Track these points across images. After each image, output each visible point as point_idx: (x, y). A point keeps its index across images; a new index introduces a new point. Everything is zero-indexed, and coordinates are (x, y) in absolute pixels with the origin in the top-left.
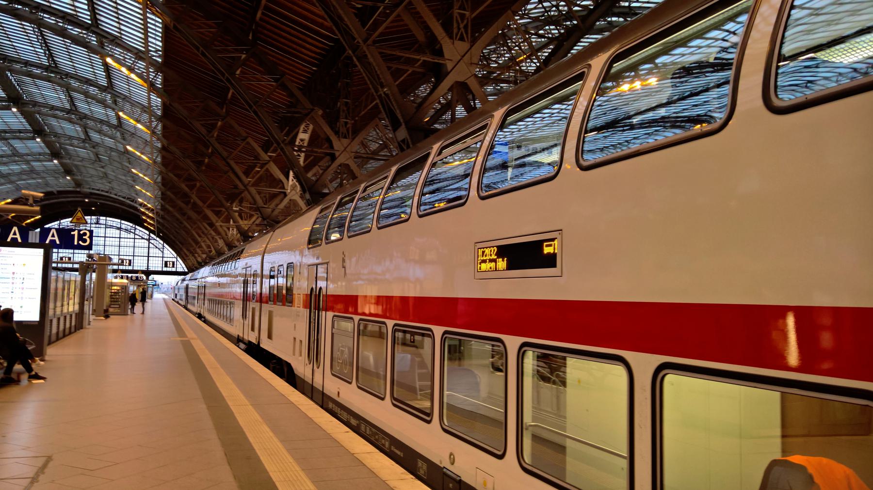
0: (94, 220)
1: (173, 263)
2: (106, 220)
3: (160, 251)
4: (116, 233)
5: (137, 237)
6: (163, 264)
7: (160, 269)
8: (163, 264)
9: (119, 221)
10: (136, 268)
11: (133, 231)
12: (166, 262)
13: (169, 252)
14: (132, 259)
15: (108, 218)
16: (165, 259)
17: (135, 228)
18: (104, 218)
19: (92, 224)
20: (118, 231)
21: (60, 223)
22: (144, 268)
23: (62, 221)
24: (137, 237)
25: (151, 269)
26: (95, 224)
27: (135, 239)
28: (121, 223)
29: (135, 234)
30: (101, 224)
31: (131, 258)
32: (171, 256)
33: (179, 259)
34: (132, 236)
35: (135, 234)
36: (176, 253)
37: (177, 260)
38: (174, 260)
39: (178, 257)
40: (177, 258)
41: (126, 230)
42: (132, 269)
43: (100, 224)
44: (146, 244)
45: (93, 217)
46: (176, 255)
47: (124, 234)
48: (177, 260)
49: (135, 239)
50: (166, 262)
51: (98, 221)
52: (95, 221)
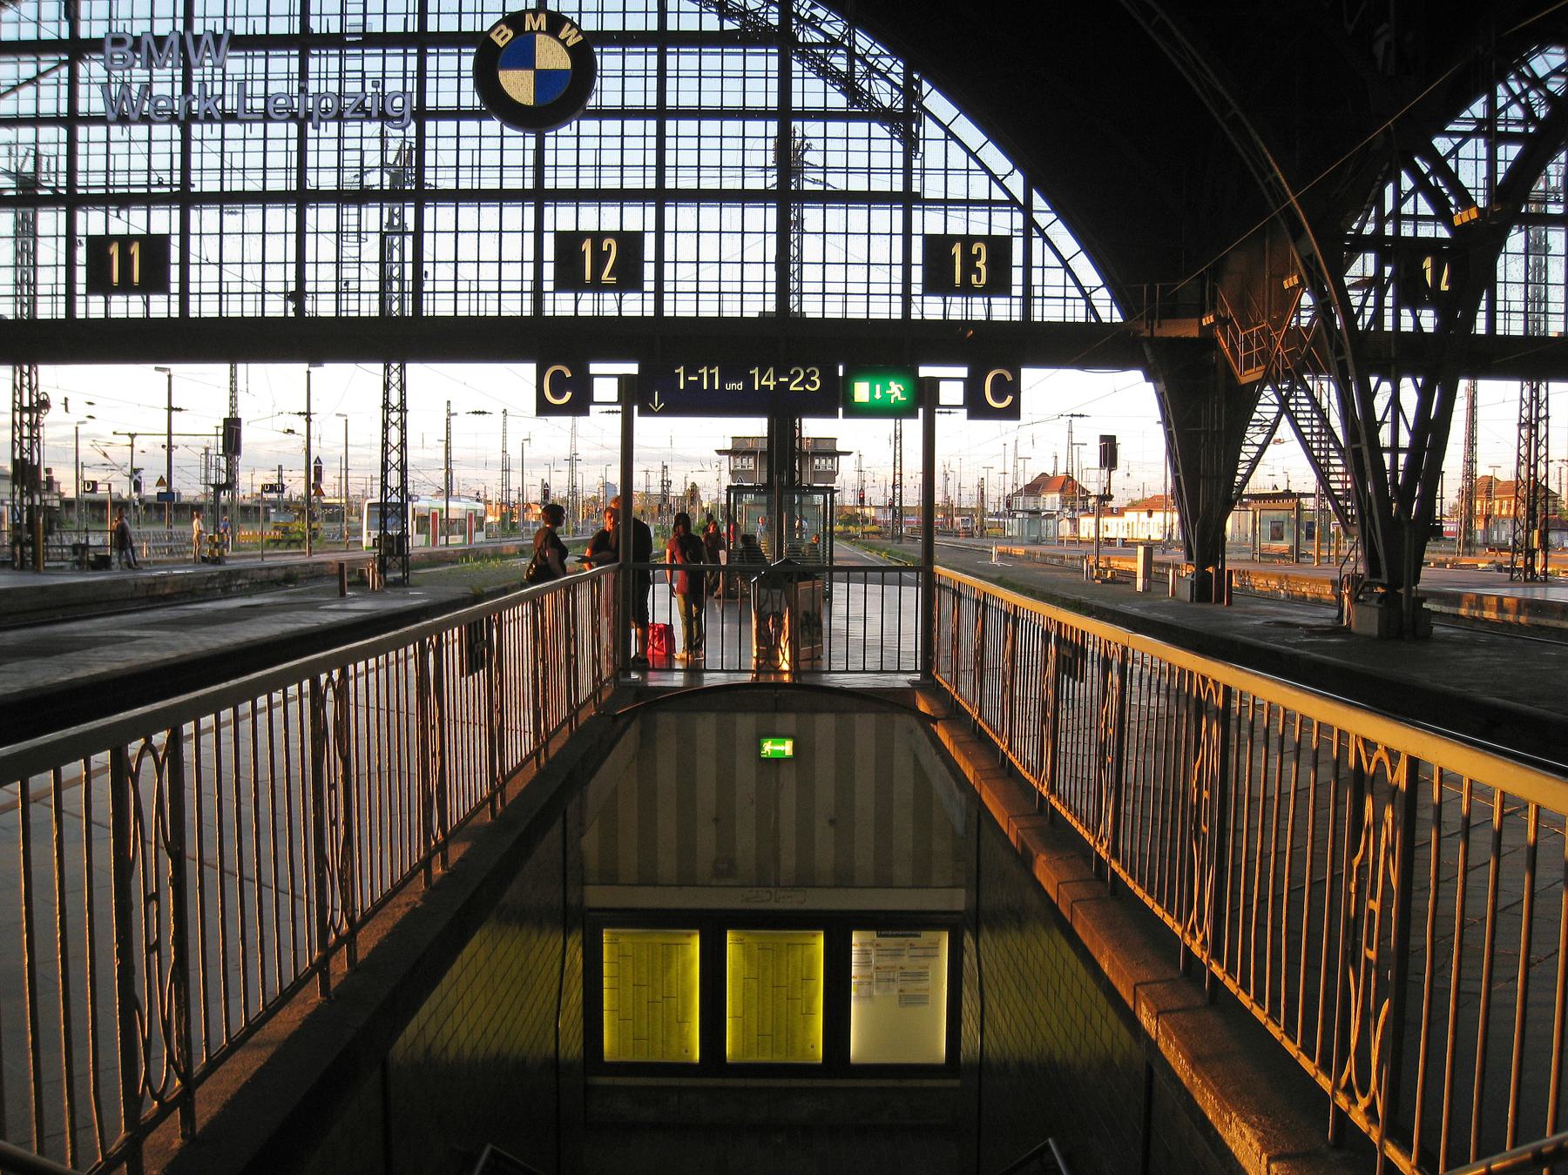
1: (999, 247)
6: (907, 264)
8: (907, 264)
13: (958, 157)
14: (651, 225)
16: (931, 222)
31: (636, 218)
32: (980, 188)
33: (1044, 215)
36: (1018, 163)
37: (1030, 223)
38: (1005, 223)
39: (1036, 197)
40: (1027, 209)
42: (650, 311)
46: (1016, 184)
48: (1030, 223)
50: (937, 246)
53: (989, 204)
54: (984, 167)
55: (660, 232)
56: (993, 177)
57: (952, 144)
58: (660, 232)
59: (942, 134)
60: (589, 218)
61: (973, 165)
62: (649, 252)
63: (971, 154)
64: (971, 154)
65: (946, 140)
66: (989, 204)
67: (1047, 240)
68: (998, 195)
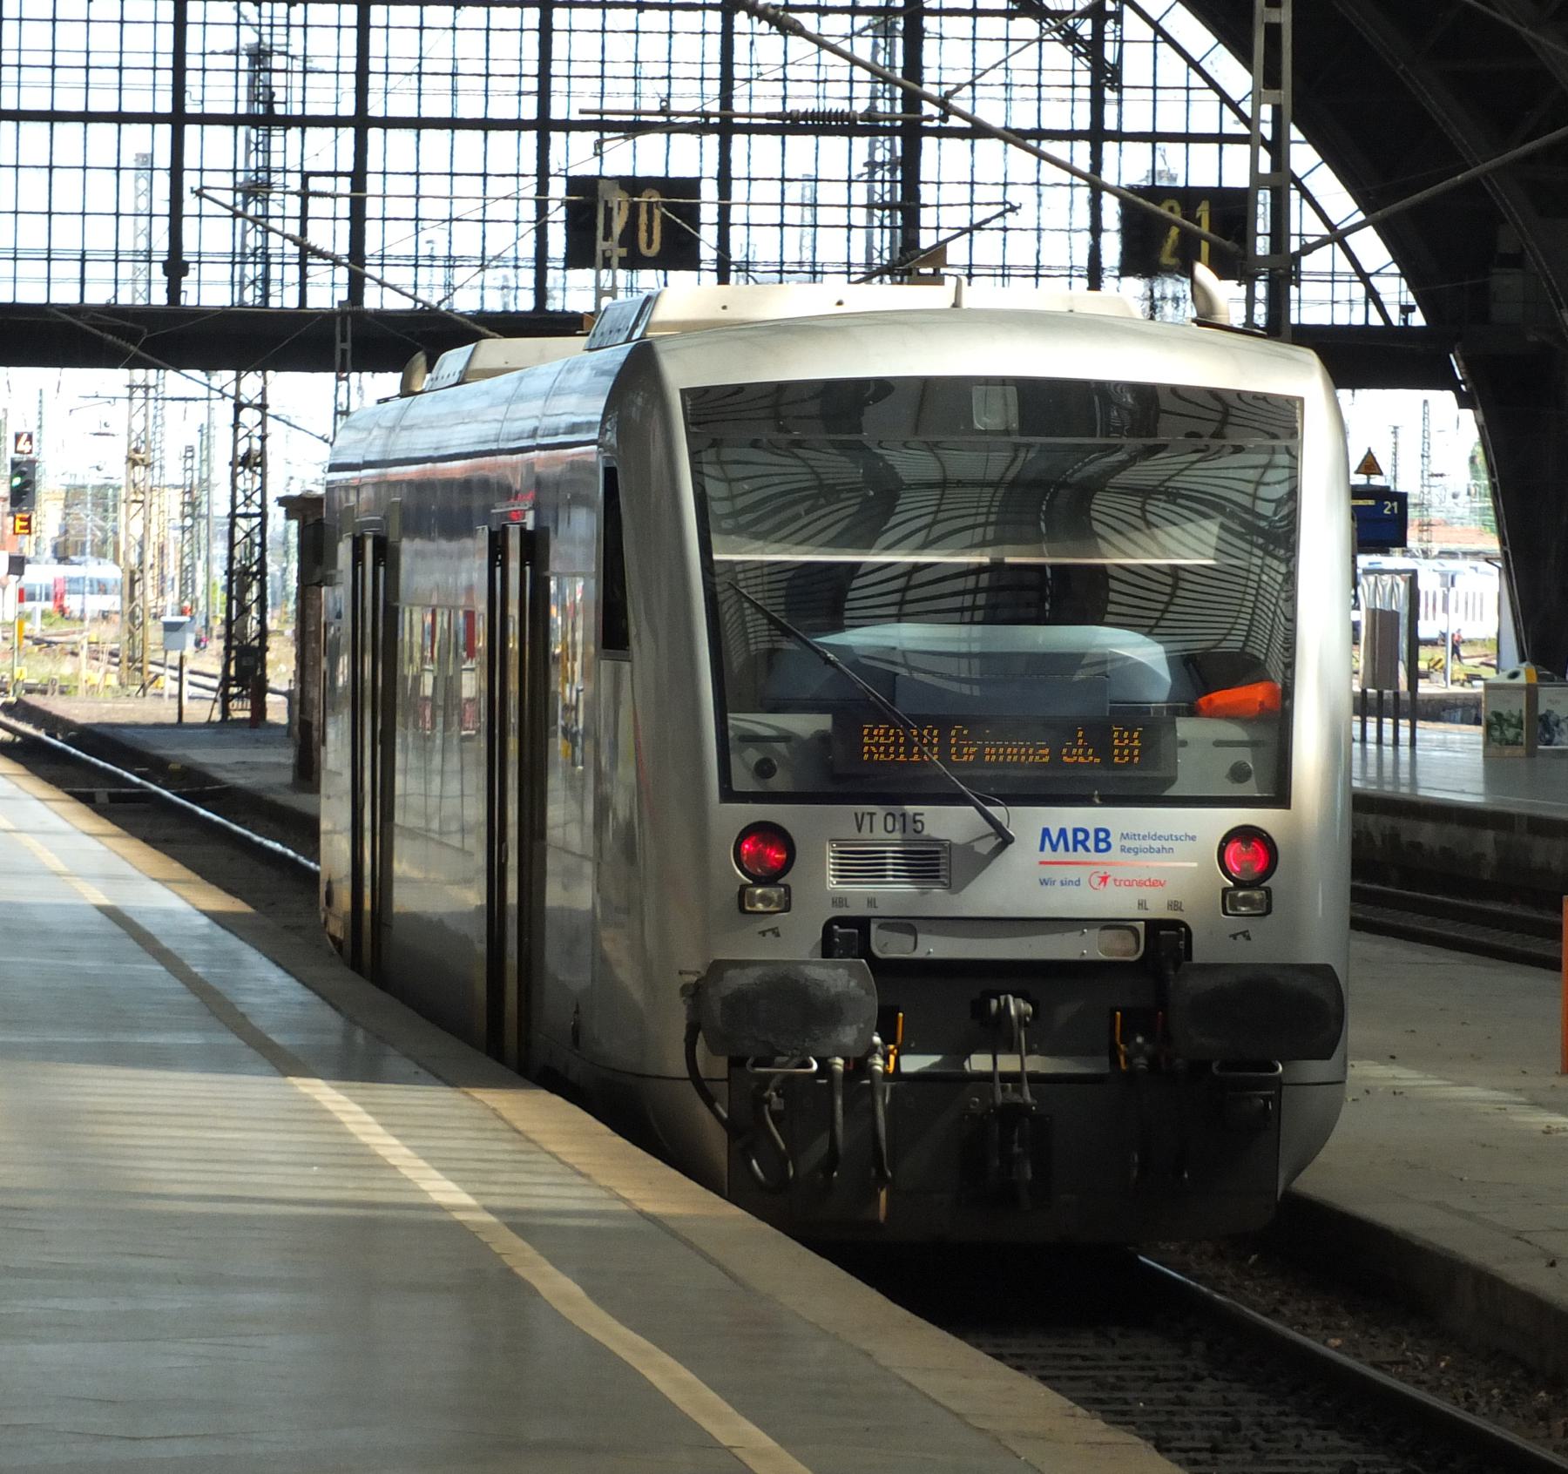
3: (1058, 54)
13: (1173, 68)
14: (712, 167)
32: (1206, 117)
33: (1303, 157)
40: (1278, 148)
53: (1221, 139)
54: (1213, 85)
55: (724, 180)
56: (1225, 99)
57: (1164, 48)
58: (724, 180)
59: (1149, 33)
60: (621, 159)
61: (1195, 80)
62: (708, 214)
63: (1193, 64)
64: (1193, 64)
65: (1155, 42)
66: (1221, 139)
67: (1306, 194)
68: (1233, 126)
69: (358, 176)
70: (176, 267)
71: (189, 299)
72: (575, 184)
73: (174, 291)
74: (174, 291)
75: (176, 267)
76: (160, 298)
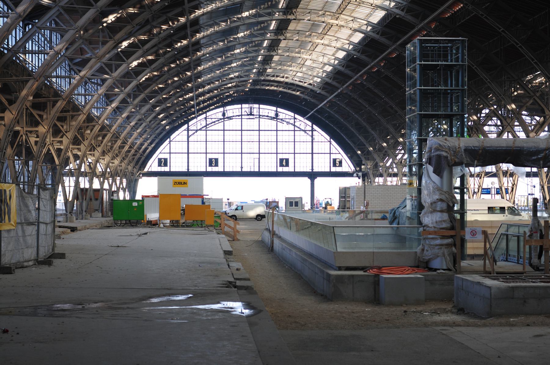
0: (246, 109)
2: (259, 108)
4: (272, 124)
5: (296, 129)
7: (327, 170)
9: (275, 108)
10: (297, 170)
11: (292, 121)
12: (335, 160)
15: (261, 106)
16: (333, 156)
17: (294, 117)
18: (256, 106)
19: (245, 115)
20: (274, 122)
21: (206, 117)
22: (309, 170)
23: (208, 114)
24: (296, 129)
25: (316, 170)
26: (248, 115)
27: (294, 131)
28: (277, 111)
29: (294, 125)
30: (253, 115)
34: (292, 128)
35: (294, 125)
41: (282, 119)
43: (253, 115)
44: (310, 139)
45: (244, 106)
47: (281, 126)
49: (294, 131)
50: (335, 160)
51: (251, 112)
52: (248, 111)
69: (259, 159)
70: (242, 168)
71: (243, 170)
72: (280, 159)
73: (242, 170)
74: (242, 170)
75: (242, 168)
76: (240, 171)
